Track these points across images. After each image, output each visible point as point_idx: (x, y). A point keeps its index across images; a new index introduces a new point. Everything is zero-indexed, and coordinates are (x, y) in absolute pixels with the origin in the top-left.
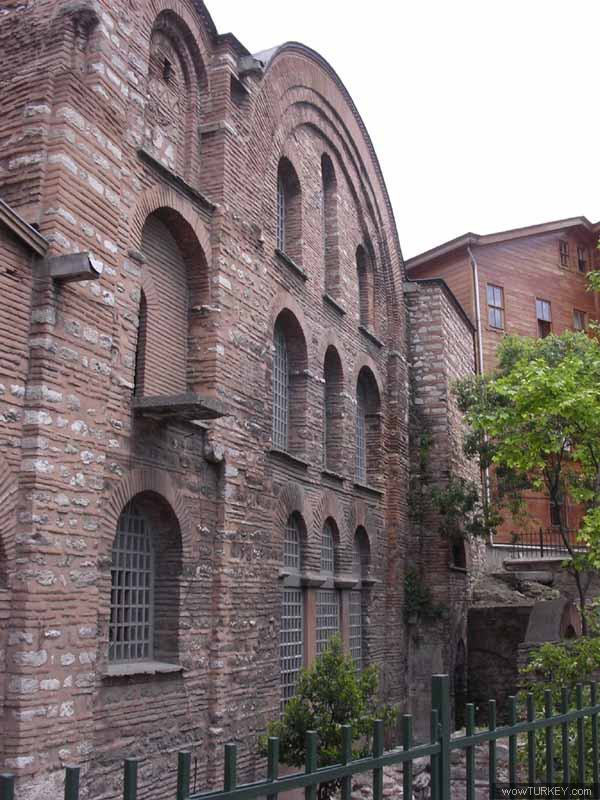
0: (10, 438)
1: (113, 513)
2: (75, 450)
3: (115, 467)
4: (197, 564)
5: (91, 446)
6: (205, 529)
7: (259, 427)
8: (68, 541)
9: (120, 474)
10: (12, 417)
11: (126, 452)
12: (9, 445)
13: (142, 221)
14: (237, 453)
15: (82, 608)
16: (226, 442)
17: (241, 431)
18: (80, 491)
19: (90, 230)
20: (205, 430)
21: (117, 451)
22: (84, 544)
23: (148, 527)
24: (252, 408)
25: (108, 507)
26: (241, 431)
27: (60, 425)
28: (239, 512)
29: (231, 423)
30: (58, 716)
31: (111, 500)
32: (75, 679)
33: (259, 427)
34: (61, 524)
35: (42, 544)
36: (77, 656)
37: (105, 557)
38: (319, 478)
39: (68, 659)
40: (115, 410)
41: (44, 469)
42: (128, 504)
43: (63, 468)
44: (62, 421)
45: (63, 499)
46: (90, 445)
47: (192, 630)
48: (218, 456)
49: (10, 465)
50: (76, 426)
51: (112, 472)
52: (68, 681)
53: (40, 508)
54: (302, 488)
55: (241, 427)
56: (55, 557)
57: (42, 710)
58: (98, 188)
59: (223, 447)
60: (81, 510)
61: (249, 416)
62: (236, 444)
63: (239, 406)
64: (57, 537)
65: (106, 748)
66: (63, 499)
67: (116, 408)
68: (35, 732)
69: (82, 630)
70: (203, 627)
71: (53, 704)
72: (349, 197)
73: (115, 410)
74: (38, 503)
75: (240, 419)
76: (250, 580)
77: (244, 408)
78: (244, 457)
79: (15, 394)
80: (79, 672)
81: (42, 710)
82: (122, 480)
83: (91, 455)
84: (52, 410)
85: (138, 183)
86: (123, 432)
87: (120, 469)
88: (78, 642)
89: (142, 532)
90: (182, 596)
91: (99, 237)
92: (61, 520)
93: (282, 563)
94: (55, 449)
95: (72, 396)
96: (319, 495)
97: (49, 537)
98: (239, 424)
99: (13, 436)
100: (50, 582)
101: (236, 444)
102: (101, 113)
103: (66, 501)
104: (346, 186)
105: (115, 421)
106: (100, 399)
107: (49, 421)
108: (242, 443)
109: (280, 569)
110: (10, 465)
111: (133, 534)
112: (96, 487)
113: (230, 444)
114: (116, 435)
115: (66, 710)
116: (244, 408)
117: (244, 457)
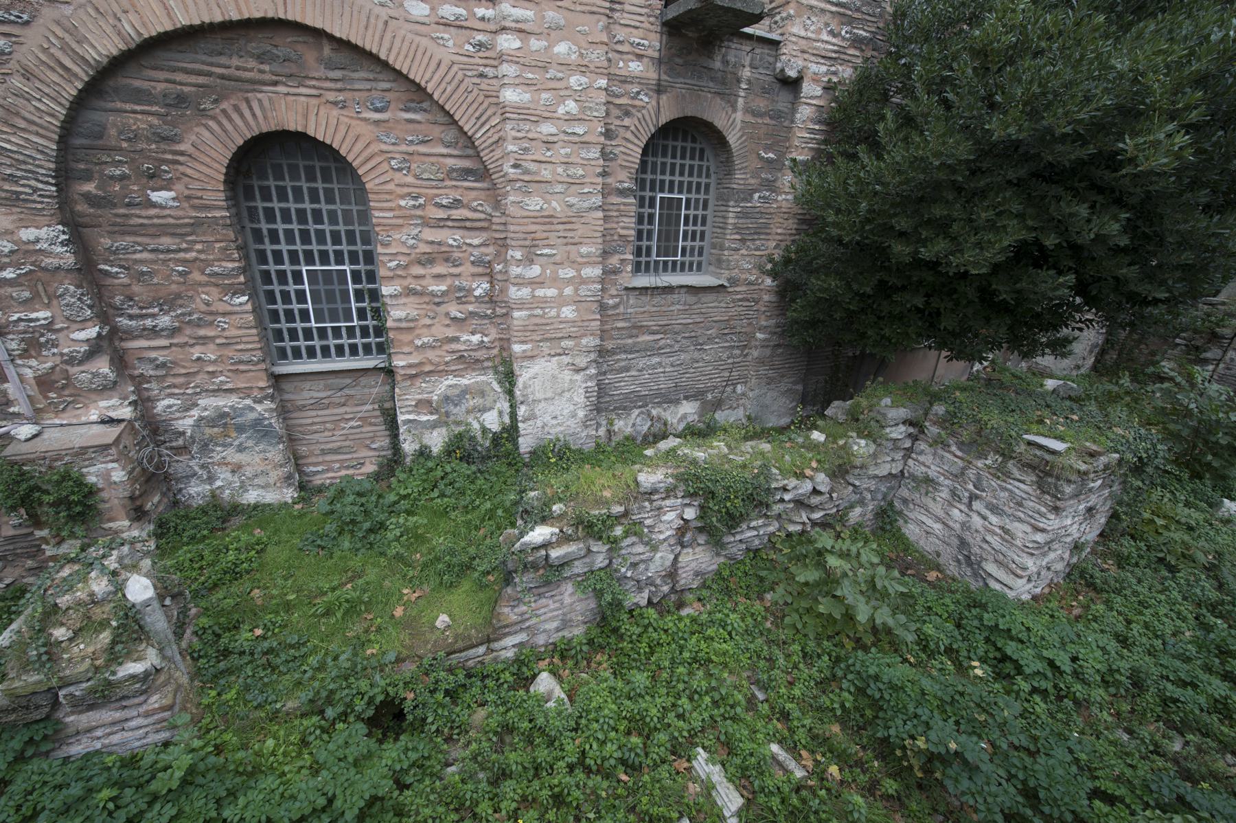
0: (481, 69)
1: (636, 141)
2: (560, 75)
3: (638, 93)
4: (755, 191)
5: (583, 69)
6: (771, 155)
7: (864, 34)
8: (560, 170)
9: (646, 100)
10: (480, 46)
11: (653, 75)
12: (481, 75)
14: (824, 69)
15: (581, 230)
16: (806, 56)
17: (834, 40)
18: (571, 119)
20: (779, 42)
21: (643, 75)
22: (581, 172)
23: (707, 153)
25: (629, 135)
26: (834, 40)
27: (534, 49)
29: (819, 31)
30: (558, 316)
31: (633, 128)
32: (576, 290)
33: (864, 34)
34: (549, 154)
35: (524, 173)
36: (578, 271)
37: (626, 185)
39: (567, 273)
40: (637, 28)
41: (517, 99)
43: (544, 95)
44: (535, 44)
45: (547, 128)
46: (583, 69)
47: (744, 252)
48: (792, 74)
49: (487, 97)
50: (561, 48)
51: (633, 98)
52: (568, 291)
53: (515, 138)
55: (834, 36)
56: (543, 185)
57: (539, 312)
59: (800, 63)
60: (576, 139)
61: (850, 21)
62: (823, 57)
63: (834, 9)
64: (543, 166)
65: (630, 341)
66: (547, 128)
67: (638, 24)
68: (531, 328)
69: (584, 250)
70: (757, 249)
71: (552, 308)
73: (637, 28)
74: (514, 133)
75: (833, 26)
77: (842, 10)
78: (835, 73)
79: (483, 19)
80: (581, 284)
81: (539, 312)
82: (649, 106)
83: (584, 80)
84: (521, 31)
86: (650, 52)
87: (646, 94)
88: (579, 260)
89: (701, 159)
90: (731, 221)
92: (548, 150)
94: (530, 76)
95: (551, 13)
97: (533, 167)
98: (831, 33)
99: (486, 66)
100: (538, 208)
101: (823, 57)
103: (553, 130)
105: (637, 41)
106: (593, 13)
107: (518, 44)
108: (834, 55)
110: (487, 97)
111: (688, 162)
112: (595, 114)
113: (813, 58)
114: (639, 57)
115: (568, 312)
116: (842, 10)
117: (835, 73)
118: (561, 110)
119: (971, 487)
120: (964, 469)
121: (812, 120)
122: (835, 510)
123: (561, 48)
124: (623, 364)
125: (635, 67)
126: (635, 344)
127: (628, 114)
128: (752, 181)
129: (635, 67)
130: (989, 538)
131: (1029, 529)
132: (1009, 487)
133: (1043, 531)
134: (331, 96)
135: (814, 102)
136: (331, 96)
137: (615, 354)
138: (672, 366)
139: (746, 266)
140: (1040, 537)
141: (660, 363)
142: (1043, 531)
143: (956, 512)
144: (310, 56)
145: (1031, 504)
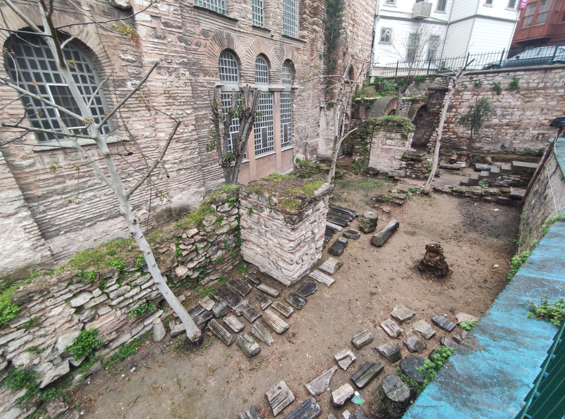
28: (159, 47)
38: (251, 29)
54: (233, 34)
76: (181, 88)
93: (217, 79)
96: (251, 40)
109: (216, 82)
119: (263, 227)
120: (259, 219)
121: (151, 36)
122: (204, 258)
124: (60, 202)
126: (65, 188)
128: (122, 74)
130: (277, 250)
131: (287, 242)
132: (275, 223)
133: (292, 241)
135: (147, 24)
137: (50, 197)
138: (105, 195)
139: (139, 127)
140: (292, 244)
141: (95, 196)
142: (292, 241)
143: (262, 240)
145: (285, 229)
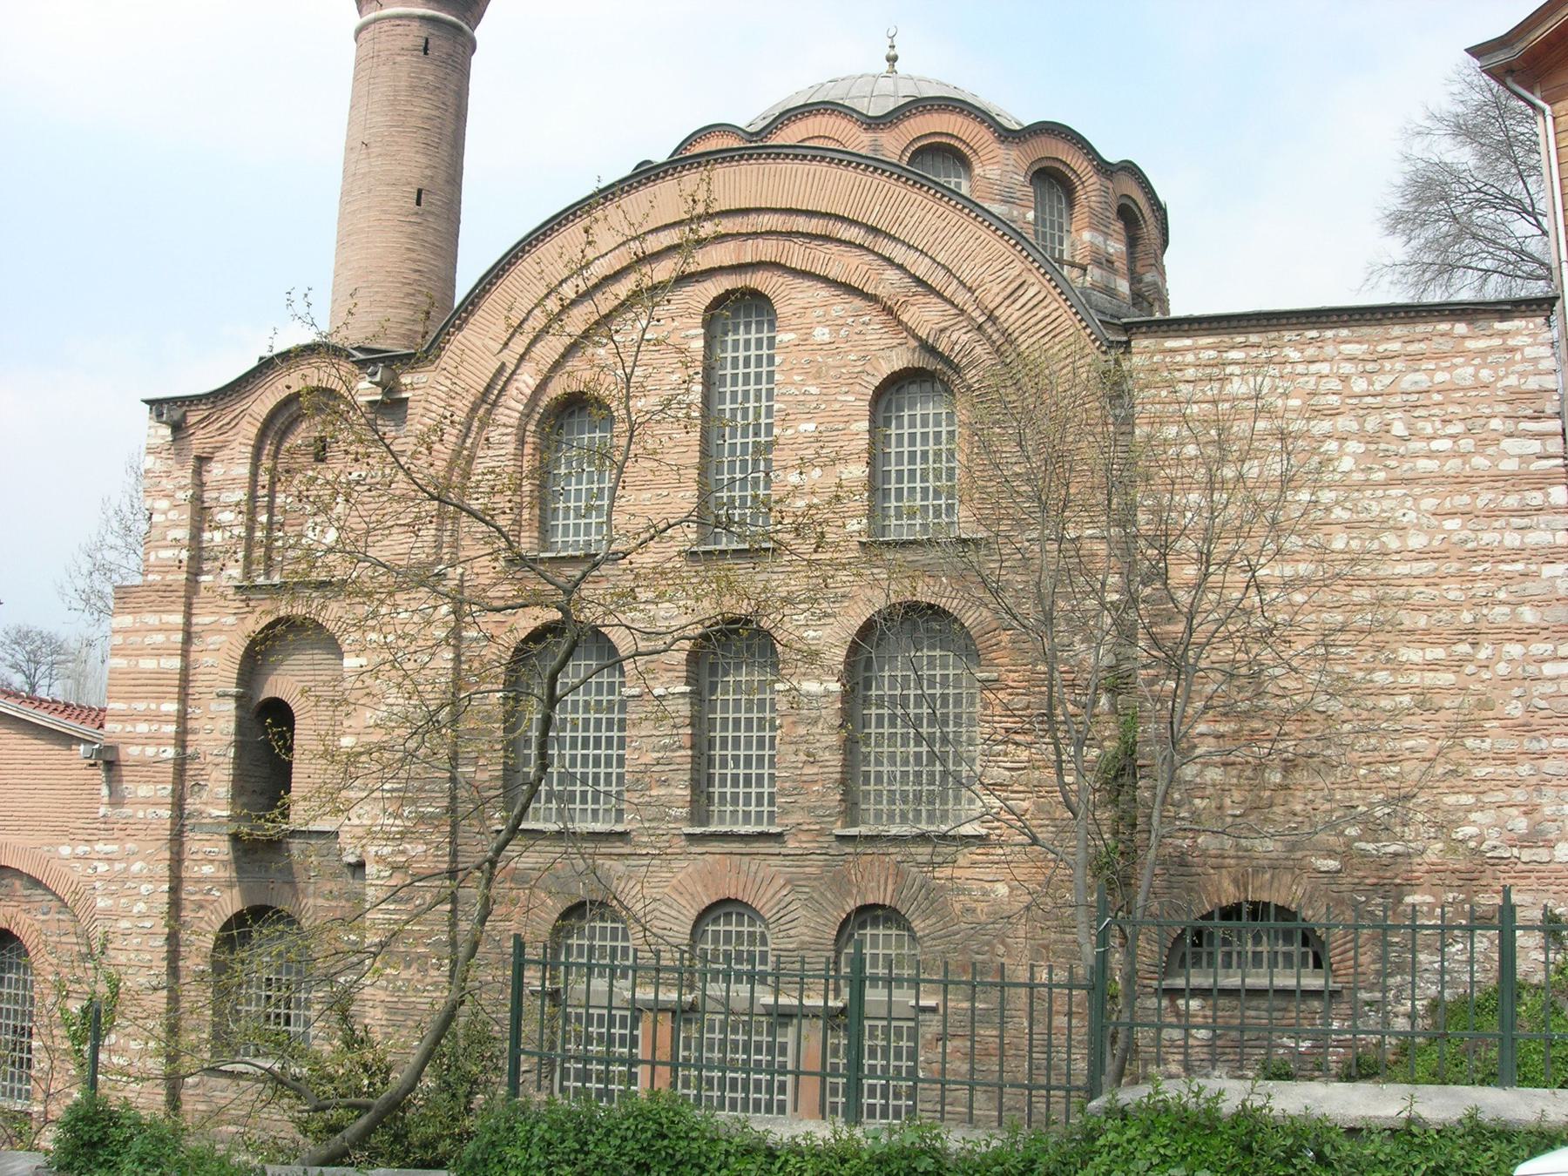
13: (239, 652)
18: (142, 916)
19: (141, 706)
24: (421, 790)
42: (229, 920)
44: (118, 866)
45: (124, 924)
58: (148, 664)
61: (414, 802)
72: (842, 306)
83: (150, 887)
85: (231, 620)
86: (220, 857)
91: (153, 706)
102: (154, 596)
103: (128, 925)
104: (822, 292)
118: (135, 910)
123: (137, 867)
125: (208, 870)
127: (201, 907)
129: (208, 870)
134: (24, 906)
136: (24, 906)
144: (18, 883)
